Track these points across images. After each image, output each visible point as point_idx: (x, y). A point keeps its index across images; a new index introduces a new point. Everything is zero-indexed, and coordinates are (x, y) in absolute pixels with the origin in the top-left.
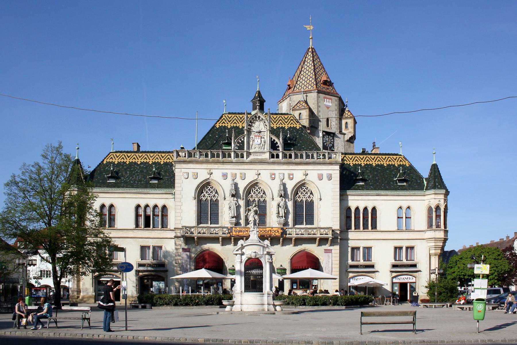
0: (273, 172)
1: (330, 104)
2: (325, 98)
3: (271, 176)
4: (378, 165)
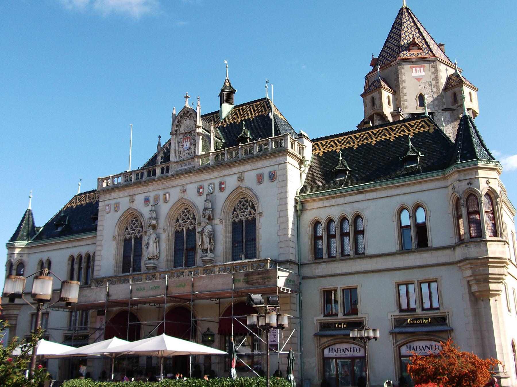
0: (200, 184)
1: (423, 74)
2: (411, 68)
3: (198, 191)
4: (381, 141)
